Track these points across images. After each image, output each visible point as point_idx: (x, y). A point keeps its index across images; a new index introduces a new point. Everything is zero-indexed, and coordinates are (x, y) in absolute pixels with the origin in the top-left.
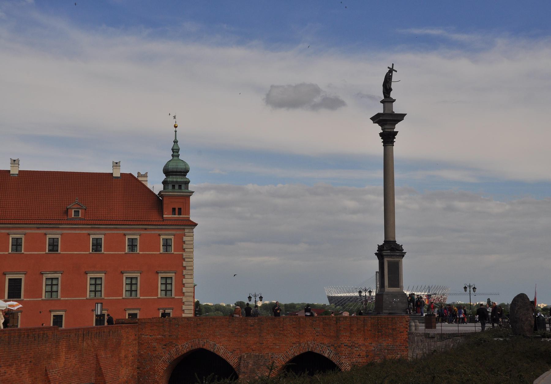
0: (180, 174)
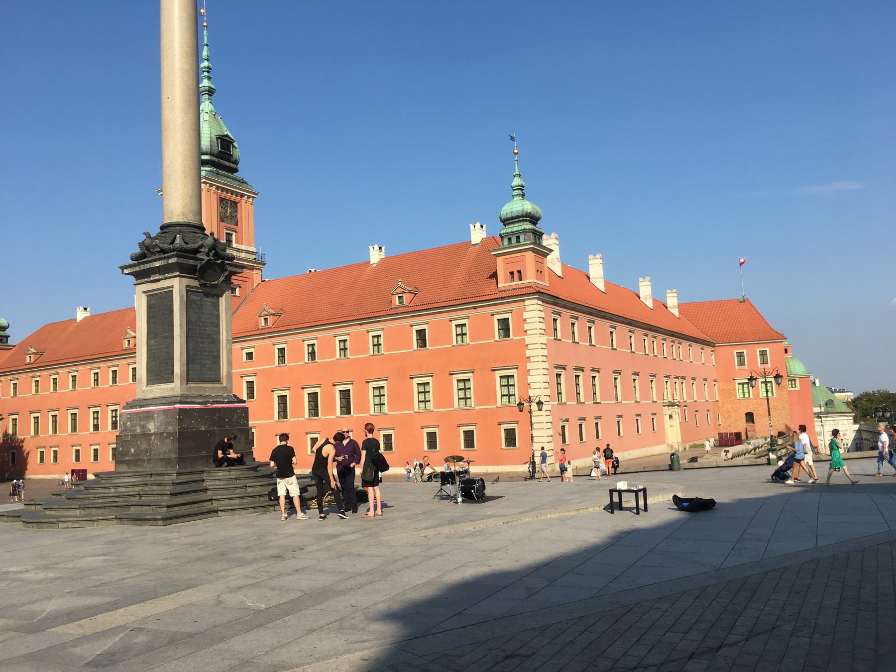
0: (518, 219)
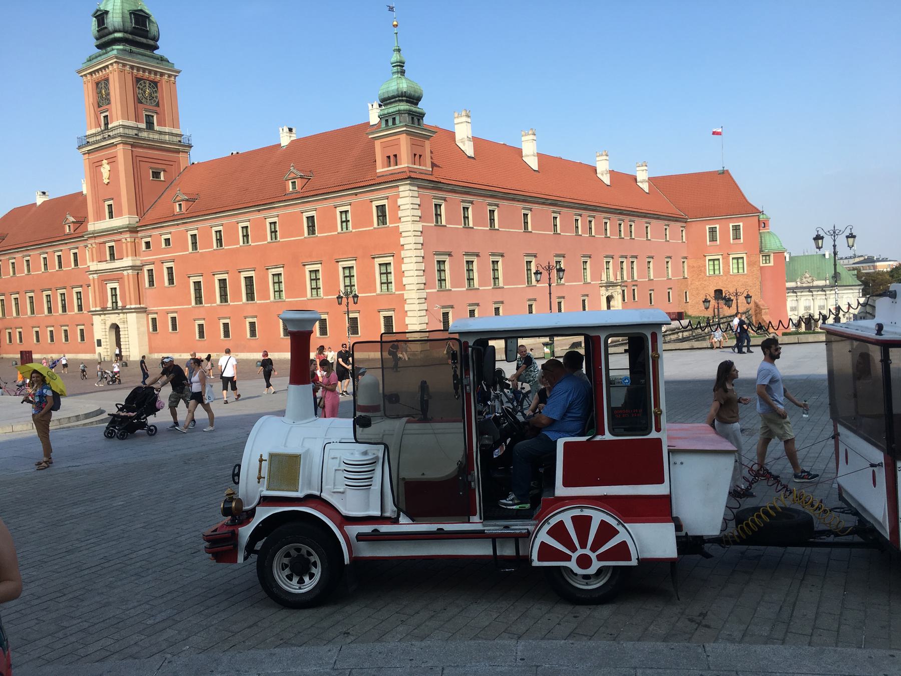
0: (394, 100)
